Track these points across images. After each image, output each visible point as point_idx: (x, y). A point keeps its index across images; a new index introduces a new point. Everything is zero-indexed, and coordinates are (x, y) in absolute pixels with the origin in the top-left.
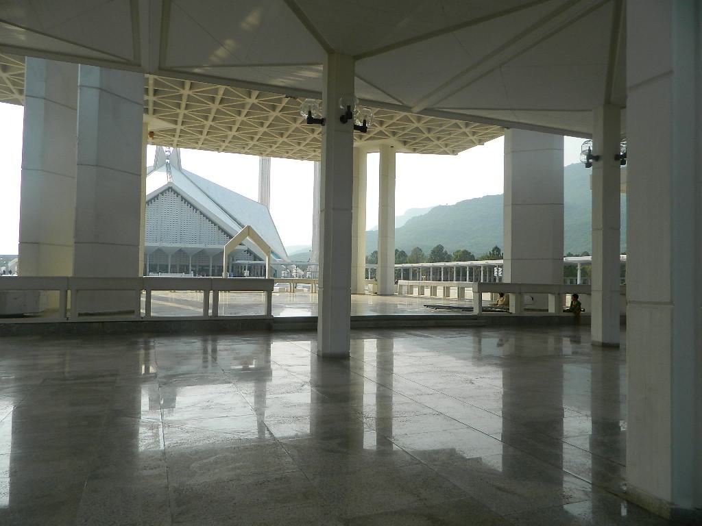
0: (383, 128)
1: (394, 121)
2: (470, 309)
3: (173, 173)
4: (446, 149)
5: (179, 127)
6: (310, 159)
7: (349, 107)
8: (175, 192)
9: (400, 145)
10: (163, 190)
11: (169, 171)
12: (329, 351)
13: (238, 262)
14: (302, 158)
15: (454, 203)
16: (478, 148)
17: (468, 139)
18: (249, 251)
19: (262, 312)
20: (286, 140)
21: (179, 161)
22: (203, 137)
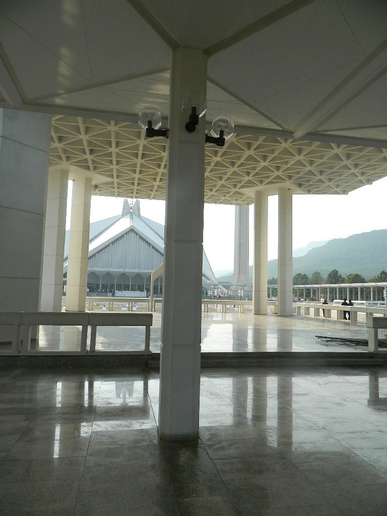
0: (280, 173)
1: (289, 166)
2: (365, 343)
3: (134, 219)
4: (337, 190)
5: (116, 180)
7: (194, 109)
8: (135, 233)
10: (128, 230)
11: (132, 218)
12: (167, 432)
14: (216, 202)
15: (346, 237)
16: (368, 186)
17: (358, 179)
19: (142, 348)
22: (135, 187)
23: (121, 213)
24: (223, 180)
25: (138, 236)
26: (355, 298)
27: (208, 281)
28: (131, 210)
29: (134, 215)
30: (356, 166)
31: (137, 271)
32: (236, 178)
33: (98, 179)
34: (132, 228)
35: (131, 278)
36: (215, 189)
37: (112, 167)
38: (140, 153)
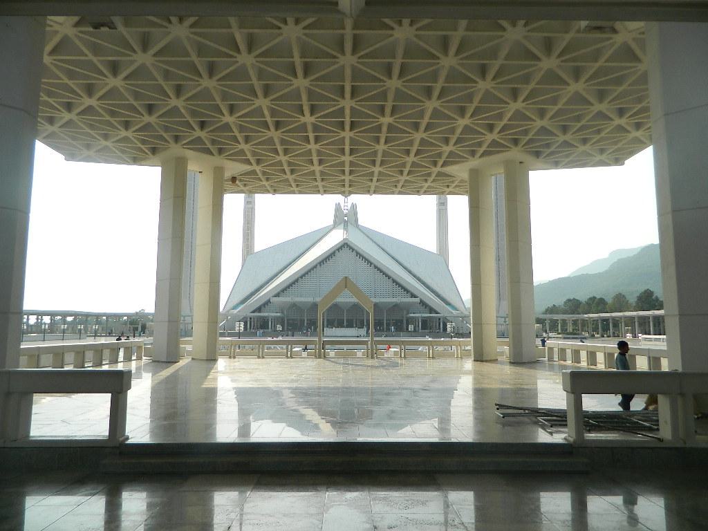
4: (604, 157)
5: (258, 169)
6: (426, 193)
10: (340, 245)
11: (345, 228)
13: (412, 315)
18: (422, 303)
21: (356, 220)
23: (331, 223)
24: (412, 154)
25: (354, 253)
26: (655, 330)
28: (346, 218)
30: (621, 112)
33: (233, 168)
35: (345, 311)
36: (406, 171)
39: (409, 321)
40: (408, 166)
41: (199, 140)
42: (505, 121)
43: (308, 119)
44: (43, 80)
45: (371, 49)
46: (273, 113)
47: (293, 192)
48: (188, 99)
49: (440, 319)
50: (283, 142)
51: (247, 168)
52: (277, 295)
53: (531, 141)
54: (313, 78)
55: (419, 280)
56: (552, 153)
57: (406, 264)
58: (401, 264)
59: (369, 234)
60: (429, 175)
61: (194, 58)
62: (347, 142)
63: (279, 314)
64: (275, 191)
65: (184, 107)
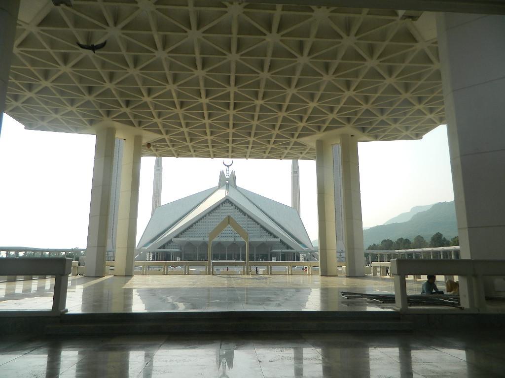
3: (230, 190)
4: (408, 133)
5: (166, 137)
6: (286, 158)
8: (231, 203)
9: (357, 133)
11: (227, 189)
13: (274, 250)
18: (281, 241)
20: (289, 151)
21: (235, 183)
23: (217, 185)
24: (277, 128)
27: (304, 248)
28: (228, 182)
29: (230, 186)
31: (232, 240)
32: (290, 126)
33: (149, 137)
34: (227, 198)
35: (226, 248)
37: (206, 138)
38: (231, 123)
39: (275, 254)
40: (274, 137)
41: (124, 115)
42: (341, 105)
43: (204, 100)
44: (12, 66)
45: (251, 49)
46: (179, 95)
47: (191, 156)
48: (118, 83)
49: (294, 254)
50: (185, 117)
51: (158, 137)
52: (177, 236)
53: (359, 120)
54: (208, 69)
55: (279, 225)
56: (374, 129)
57: (270, 214)
58: (267, 215)
59: (244, 193)
60: (288, 144)
61: (124, 52)
62: (231, 118)
63: (178, 250)
64: (178, 155)
65: (116, 90)
